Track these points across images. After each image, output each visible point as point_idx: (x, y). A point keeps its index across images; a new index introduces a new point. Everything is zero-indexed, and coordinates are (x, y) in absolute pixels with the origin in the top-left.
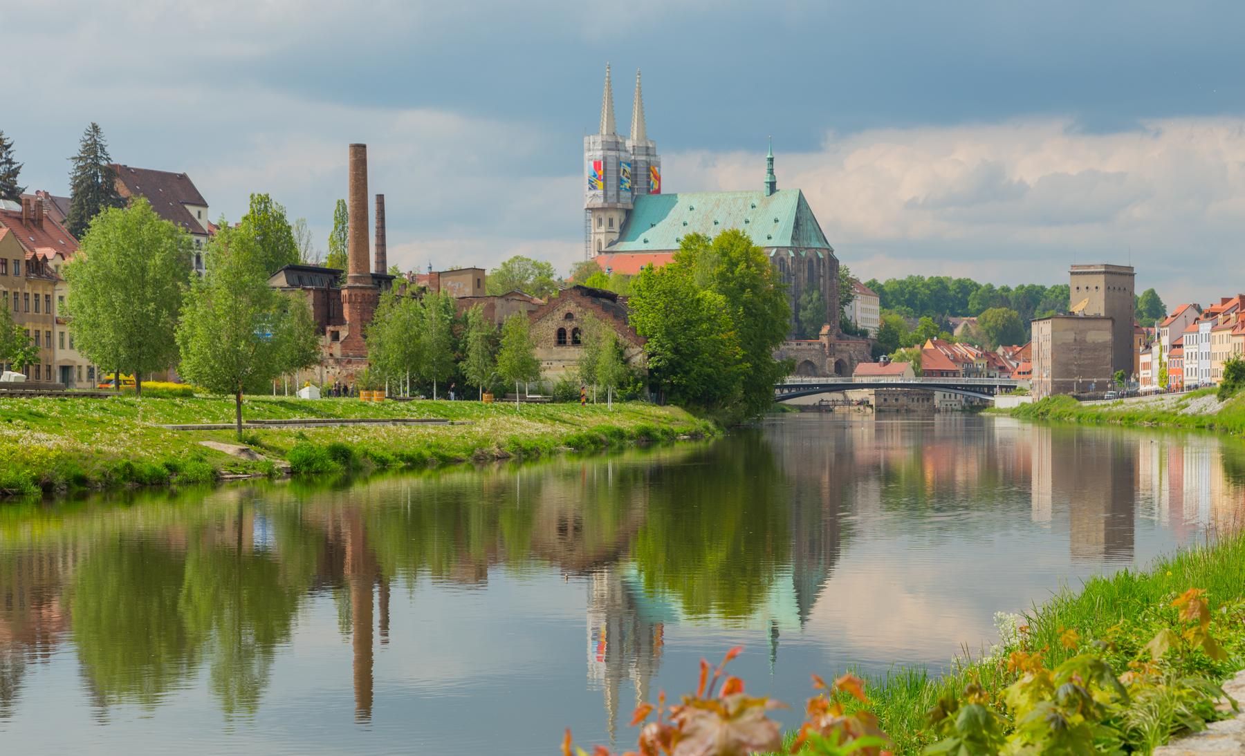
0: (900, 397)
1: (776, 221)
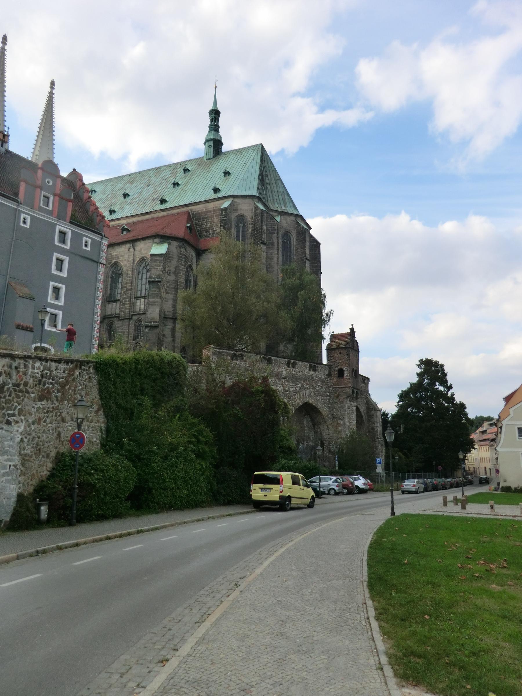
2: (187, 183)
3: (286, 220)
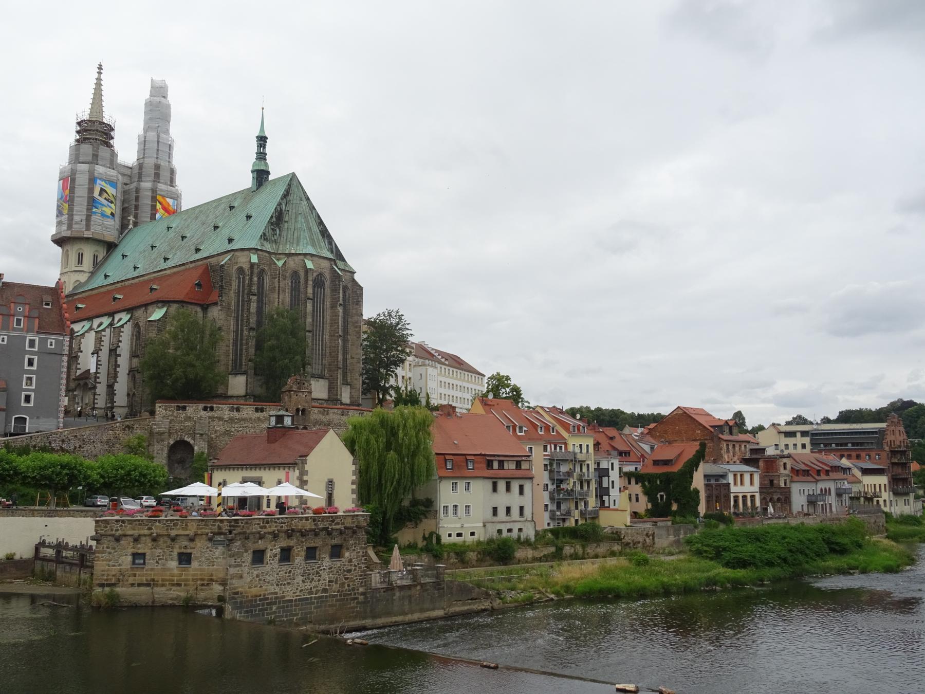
0: (199, 548)
1: (249, 217)
3: (294, 260)
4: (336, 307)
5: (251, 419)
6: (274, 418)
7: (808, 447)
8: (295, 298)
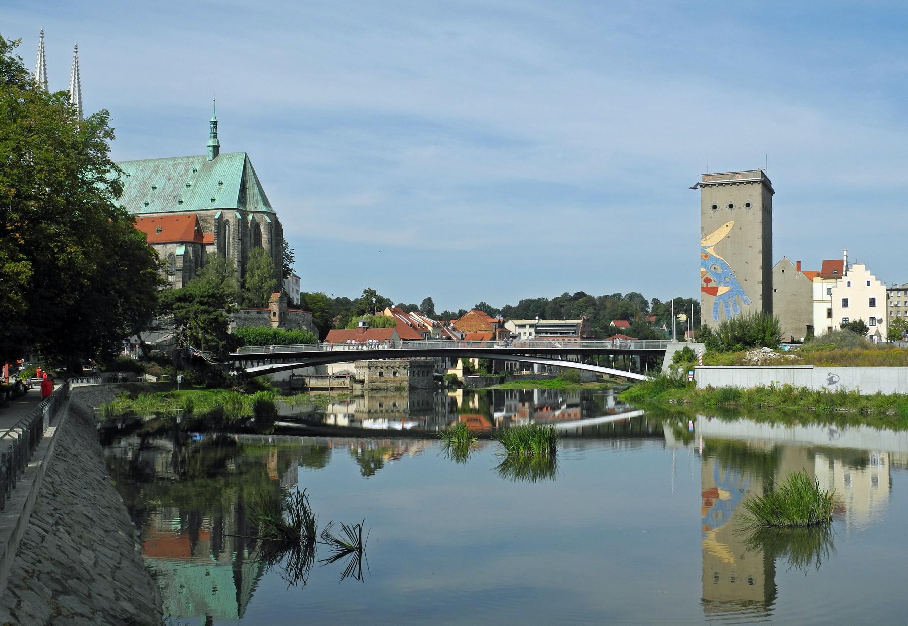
1: (221, 183)
2: (195, 185)
4: (279, 245)
5: (255, 318)
6: (362, 323)
7: (533, 335)
8: (257, 240)
